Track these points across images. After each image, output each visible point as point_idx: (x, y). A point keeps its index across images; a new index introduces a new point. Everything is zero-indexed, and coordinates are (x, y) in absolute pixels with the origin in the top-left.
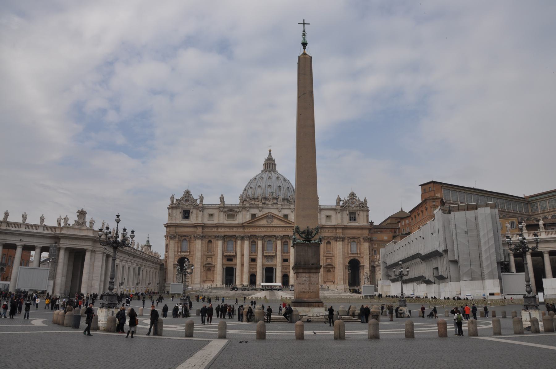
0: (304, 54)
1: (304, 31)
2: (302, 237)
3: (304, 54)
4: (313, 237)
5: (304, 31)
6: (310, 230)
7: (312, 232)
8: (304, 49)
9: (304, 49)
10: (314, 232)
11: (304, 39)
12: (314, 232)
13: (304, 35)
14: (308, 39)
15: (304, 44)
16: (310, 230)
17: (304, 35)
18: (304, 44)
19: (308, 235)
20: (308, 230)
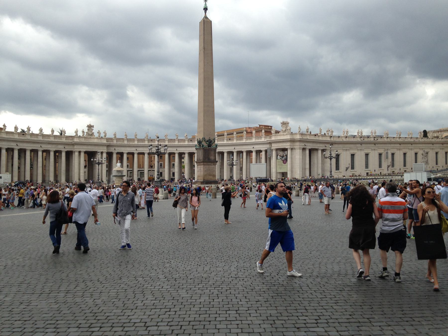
0: (206, 17)
8: (205, 12)
9: (205, 12)
10: (213, 141)
11: (206, 5)
15: (206, 9)
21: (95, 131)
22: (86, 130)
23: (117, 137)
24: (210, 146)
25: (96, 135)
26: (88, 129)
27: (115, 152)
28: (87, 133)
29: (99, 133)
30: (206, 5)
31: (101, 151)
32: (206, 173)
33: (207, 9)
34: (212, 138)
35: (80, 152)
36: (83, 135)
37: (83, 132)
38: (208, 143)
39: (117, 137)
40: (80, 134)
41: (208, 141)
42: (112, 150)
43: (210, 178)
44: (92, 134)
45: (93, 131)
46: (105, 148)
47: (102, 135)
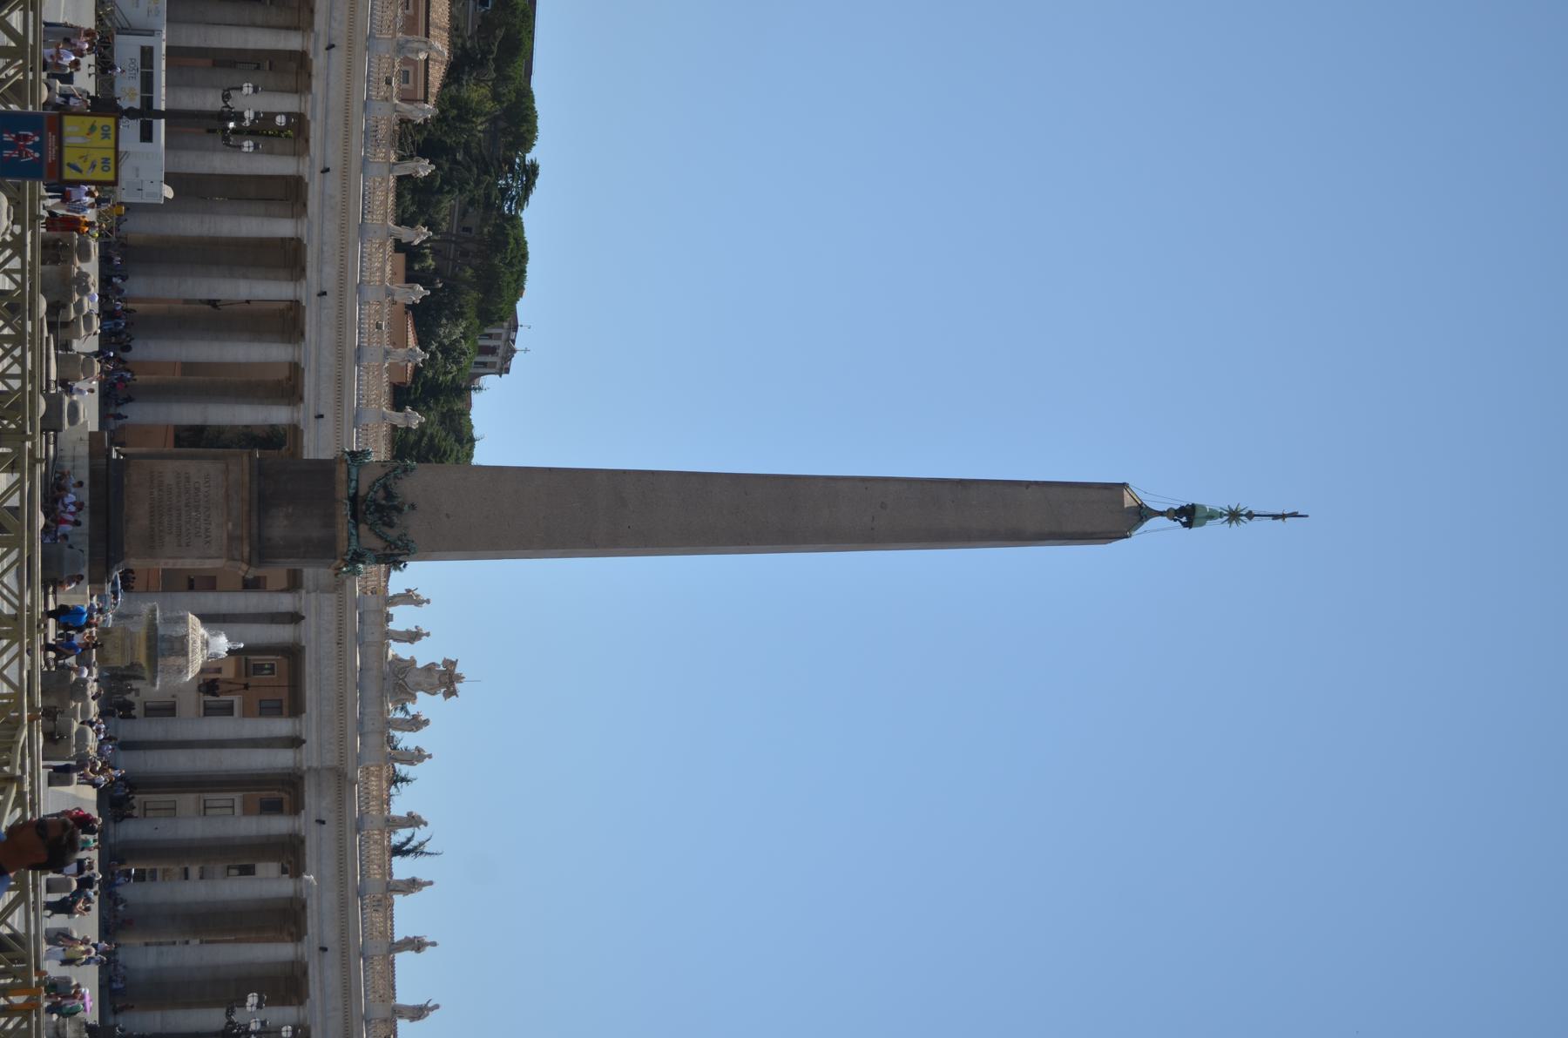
0: (1142, 513)
1: (1250, 515)
2: (371, 488)
3: (1142, 513)
5: (1250, 515)
7: (391, 525)
10: (392, 534)
11: (1212, 516)
12: (392, 534)
13: (1234, 516)
14: (1212, 527)
15: (1189, 515)
17: (1234, 516)
18: (1189, 515)
19: (380, 509)
20: (399, 510)
21: (424, 704)
22: (422, 654)
26: (430, 668)
28: (413, 661)
29: (416, 723)
30: (1212, 516)
31: (312, 738)
33: (1188, 525)
35: (295, 618)
37: (413, 636)
38: (381, 493)
39: (398, 899)
40: (402, 619)
41: (389, 495)
42: (315, 800)
45: (420, 694)
46: (330, 759)
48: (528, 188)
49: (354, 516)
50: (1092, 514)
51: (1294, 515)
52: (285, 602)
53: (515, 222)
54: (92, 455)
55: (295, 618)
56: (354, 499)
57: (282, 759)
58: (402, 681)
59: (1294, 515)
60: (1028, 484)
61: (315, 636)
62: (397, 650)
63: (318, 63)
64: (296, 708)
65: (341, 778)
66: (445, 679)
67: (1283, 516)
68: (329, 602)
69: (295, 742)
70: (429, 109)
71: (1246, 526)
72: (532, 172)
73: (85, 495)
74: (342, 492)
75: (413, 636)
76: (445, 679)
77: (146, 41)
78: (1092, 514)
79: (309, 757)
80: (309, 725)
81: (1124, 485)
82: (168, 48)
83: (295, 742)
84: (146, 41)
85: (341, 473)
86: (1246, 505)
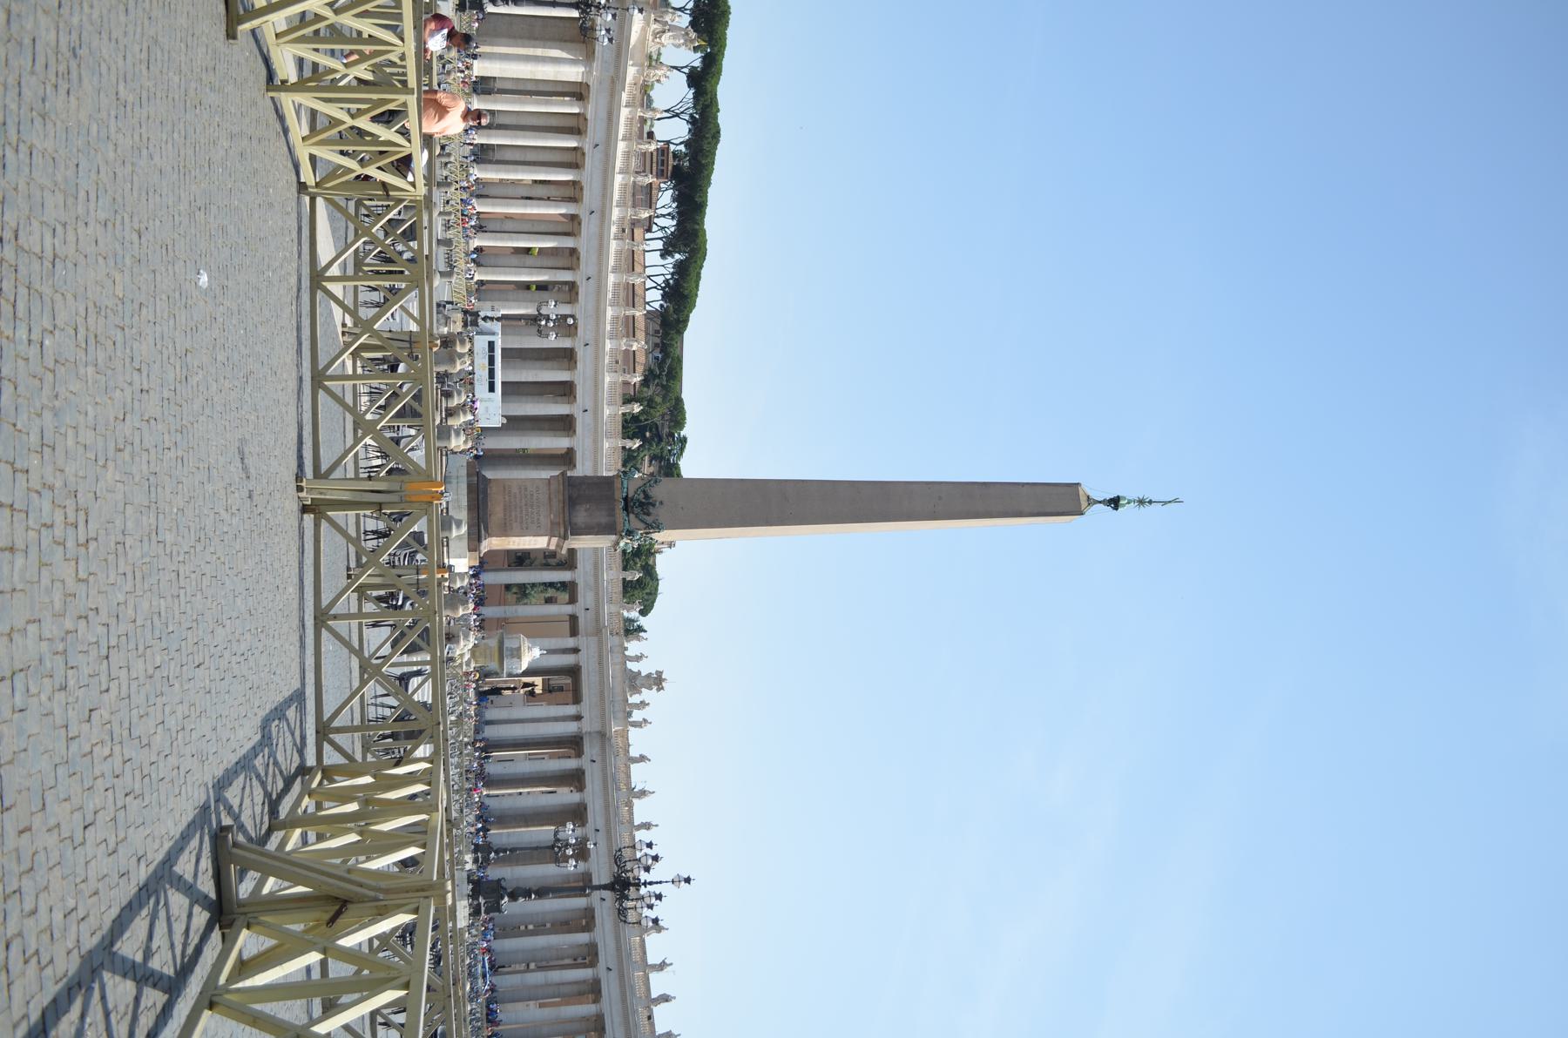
0: (1091, 502)
1: (1150, 502)
3: (1091, 502)
4: (637, 516)
5: (1150, 502)
6: (651, 509)
7: (648, 514)
10: (649, 519)
12: (649, 519)
13: (1141, 502)
15: (1115, 503)
16: (651, 509)
17: (1141, 502)
18: (1115, 503)
19: (642, 505)
21: (646, 694)
22: (644, 668)
23: (634, 767)
24: (628, 505)
25: (634, 699)
26: (649, 676)
27: (584, 763)
29: (643, 704)
32: (515, 490)
34: (660, 513)
35: (576, 651)
36: (632, 659)
37: (638, 658)
41: (647, 496)
42: (591, 750)
43: (496, 512)
44: (635, 689)
46: (596, 727)
47: (637, 716)
48: (682, 449)
49: (626, 508)
50: (1059, 500)
51: (1175, 501)
52: (570, 642)
53: (676, 466)
54: (469, 475)
55: (576, 651)
56: (626, 499)
57: (570, 728)
58: (635, 682)
59: (1175, 501)
60: (1023, 484)
61: (587, 661)
62: (632, 666)
63: (581, 353)
64: (577, 700)
65: (603, 736)
66: (657, 681)
67: (1165, 503)
68: (593, 641)
69: (578, 718)
70: (637, 379)
71: (1148, 508)
72: (684, 441)
73: (464, 529)
74: (619, 495)
75: (638, 658)
76: (657, 681)
77: (491, 338)
78: (1059, 500)
79: (587, 726)
80: (585, 708)
81: (1078, 484)
82: (503, 350)
83: (578, 718)
84: (491, 338)
85: (617, 484)
86: (1148, 496)
